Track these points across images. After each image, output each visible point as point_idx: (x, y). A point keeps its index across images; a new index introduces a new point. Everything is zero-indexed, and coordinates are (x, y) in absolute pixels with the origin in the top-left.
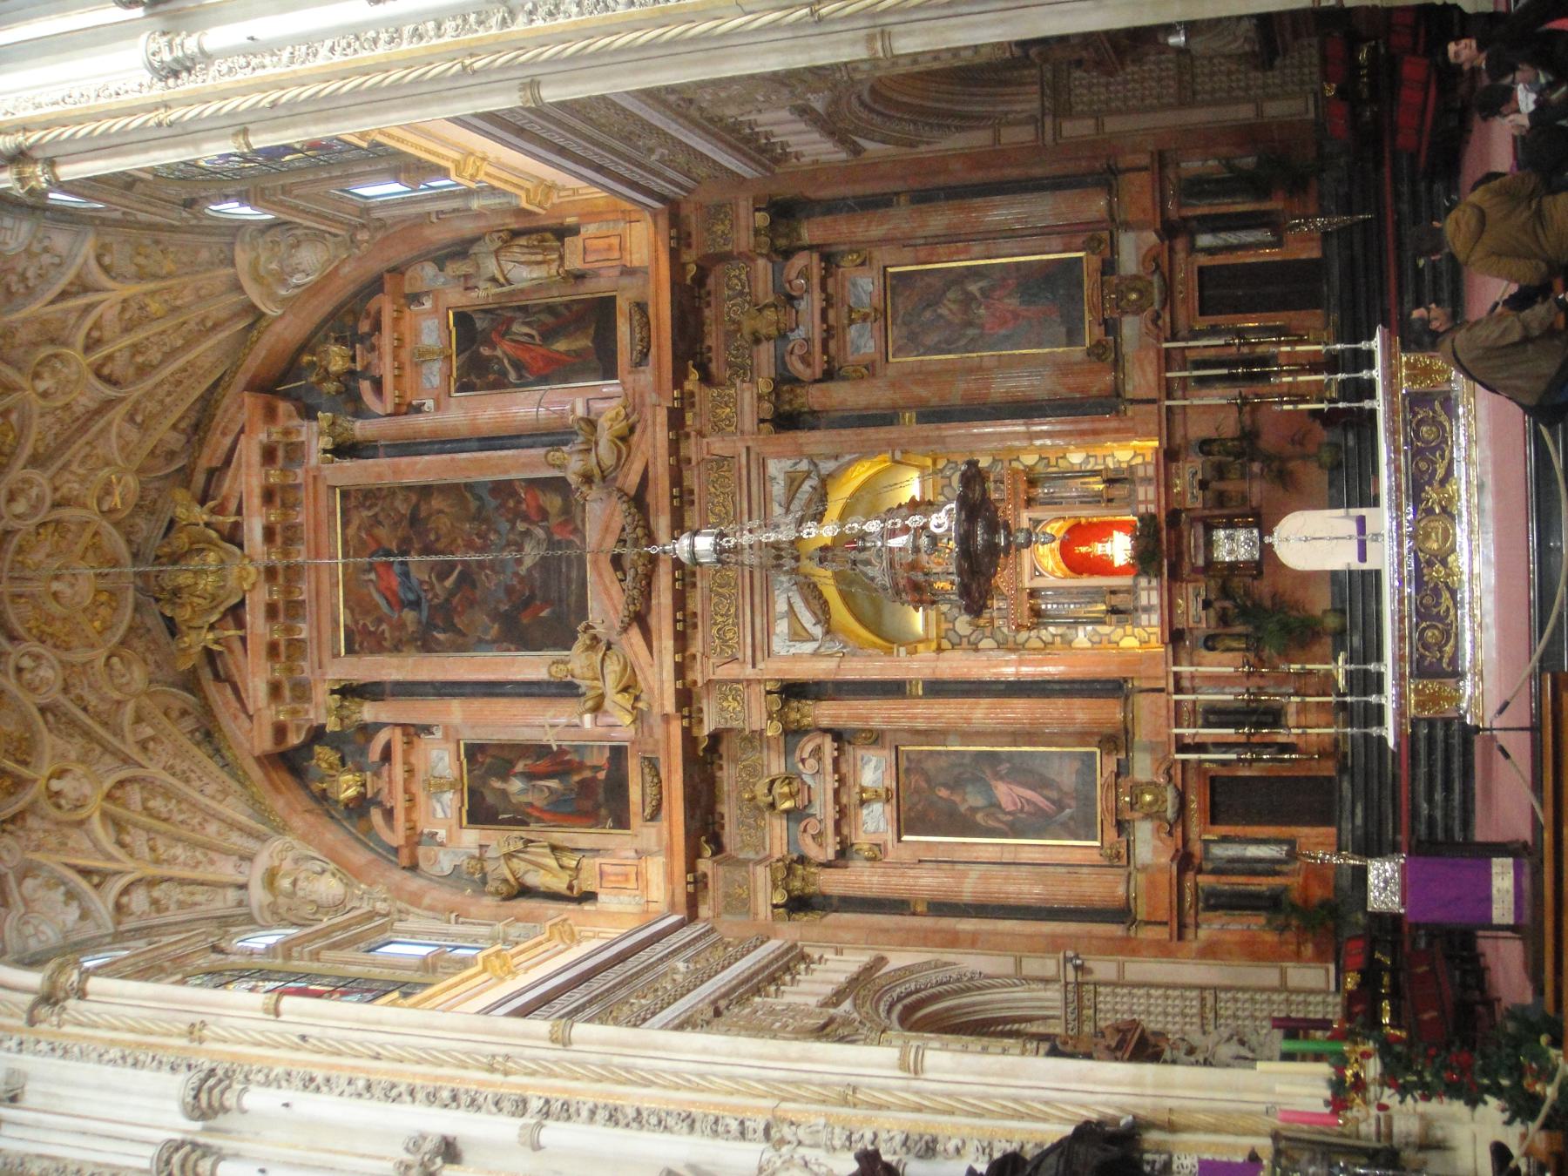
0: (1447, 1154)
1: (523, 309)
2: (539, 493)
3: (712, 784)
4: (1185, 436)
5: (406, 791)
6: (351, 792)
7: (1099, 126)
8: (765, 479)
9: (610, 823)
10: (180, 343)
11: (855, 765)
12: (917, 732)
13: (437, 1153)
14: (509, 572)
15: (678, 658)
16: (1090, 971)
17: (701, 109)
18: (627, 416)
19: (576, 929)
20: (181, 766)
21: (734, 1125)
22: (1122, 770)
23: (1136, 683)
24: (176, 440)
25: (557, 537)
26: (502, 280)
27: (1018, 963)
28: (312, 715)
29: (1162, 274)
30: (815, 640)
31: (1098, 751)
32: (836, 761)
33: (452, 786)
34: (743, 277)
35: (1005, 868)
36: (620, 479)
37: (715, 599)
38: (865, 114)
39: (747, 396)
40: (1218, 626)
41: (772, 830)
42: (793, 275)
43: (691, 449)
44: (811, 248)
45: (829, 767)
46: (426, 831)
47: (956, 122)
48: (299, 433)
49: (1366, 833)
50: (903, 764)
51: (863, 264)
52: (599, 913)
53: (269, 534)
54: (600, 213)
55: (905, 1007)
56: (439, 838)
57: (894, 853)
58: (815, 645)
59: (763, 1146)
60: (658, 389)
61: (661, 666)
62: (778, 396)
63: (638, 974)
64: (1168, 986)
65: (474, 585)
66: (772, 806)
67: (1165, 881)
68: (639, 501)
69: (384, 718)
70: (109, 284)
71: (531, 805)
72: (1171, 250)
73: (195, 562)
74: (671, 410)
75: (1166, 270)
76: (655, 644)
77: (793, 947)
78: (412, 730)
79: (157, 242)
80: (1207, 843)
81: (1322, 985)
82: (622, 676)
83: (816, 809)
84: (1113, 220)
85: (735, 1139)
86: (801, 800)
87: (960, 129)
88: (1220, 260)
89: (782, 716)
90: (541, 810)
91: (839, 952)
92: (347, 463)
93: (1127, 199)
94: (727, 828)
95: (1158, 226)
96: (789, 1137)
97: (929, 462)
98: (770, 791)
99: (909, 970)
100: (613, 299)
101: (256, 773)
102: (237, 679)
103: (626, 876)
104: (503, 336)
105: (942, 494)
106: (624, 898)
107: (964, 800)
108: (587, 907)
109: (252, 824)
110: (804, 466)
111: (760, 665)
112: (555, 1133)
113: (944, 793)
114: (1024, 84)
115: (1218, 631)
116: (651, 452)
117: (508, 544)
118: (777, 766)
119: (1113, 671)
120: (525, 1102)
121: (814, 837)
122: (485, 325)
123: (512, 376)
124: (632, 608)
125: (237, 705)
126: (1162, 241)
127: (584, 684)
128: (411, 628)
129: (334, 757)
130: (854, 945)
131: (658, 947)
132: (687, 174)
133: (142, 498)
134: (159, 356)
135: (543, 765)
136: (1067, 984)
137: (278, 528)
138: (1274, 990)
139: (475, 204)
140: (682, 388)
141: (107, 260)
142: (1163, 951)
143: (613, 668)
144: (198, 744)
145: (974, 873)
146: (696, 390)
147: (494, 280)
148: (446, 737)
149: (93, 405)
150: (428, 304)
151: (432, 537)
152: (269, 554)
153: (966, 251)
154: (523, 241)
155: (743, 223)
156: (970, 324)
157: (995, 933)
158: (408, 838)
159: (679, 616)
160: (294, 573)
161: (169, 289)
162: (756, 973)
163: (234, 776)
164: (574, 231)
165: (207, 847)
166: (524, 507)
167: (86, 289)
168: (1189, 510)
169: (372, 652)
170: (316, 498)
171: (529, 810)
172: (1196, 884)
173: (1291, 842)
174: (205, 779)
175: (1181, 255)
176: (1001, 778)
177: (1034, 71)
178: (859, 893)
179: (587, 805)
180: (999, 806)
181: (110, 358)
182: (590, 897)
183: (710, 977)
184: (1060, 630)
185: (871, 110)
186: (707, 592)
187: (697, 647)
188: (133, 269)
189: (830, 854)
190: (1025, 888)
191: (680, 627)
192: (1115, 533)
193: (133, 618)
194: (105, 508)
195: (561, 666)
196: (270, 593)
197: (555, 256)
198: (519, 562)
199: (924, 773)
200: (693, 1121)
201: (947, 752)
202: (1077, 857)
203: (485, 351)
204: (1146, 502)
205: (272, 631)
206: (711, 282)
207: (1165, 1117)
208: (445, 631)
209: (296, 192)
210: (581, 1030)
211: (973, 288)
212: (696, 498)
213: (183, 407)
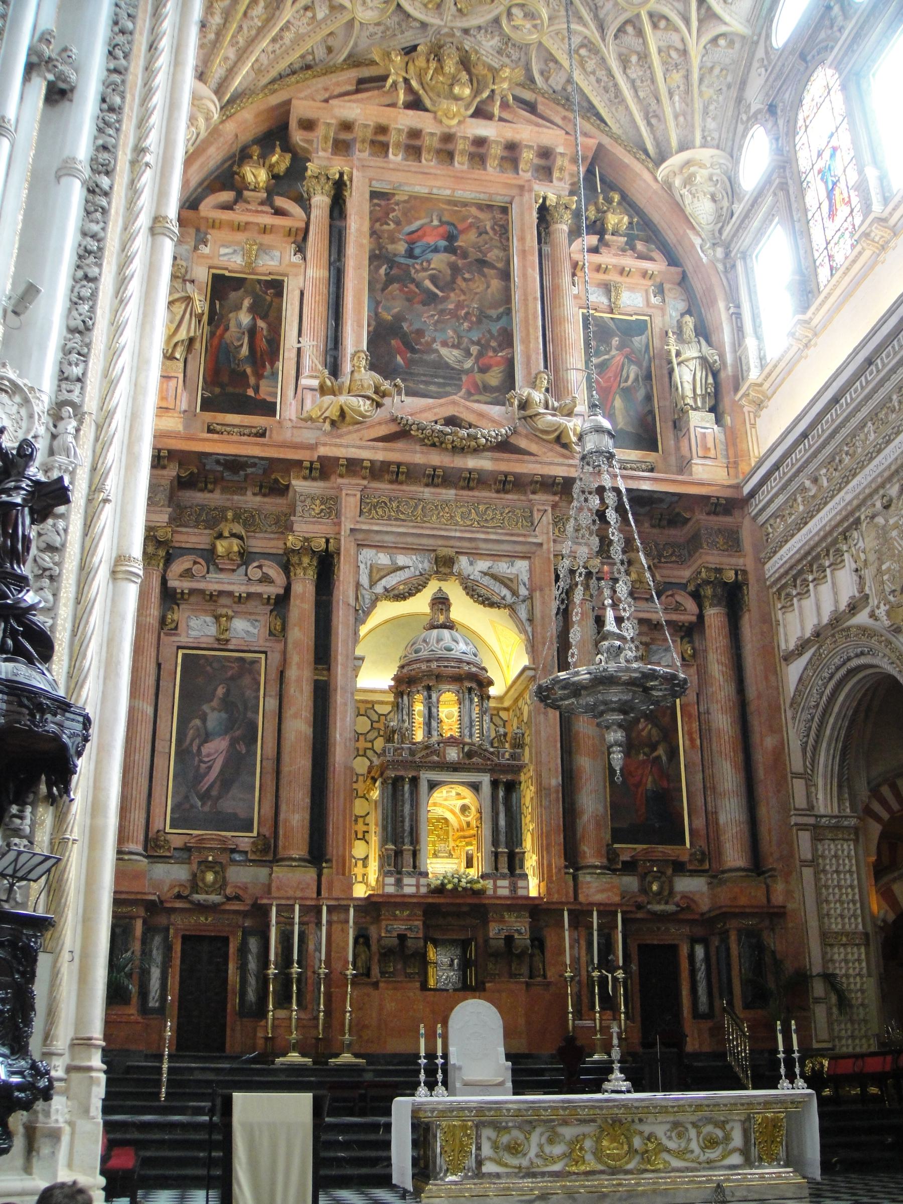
1: (648, 377)
2: (502, 368)
5: (247, 223)
6: (250, 178)
7: (805, 863)
8: (512, 557)
9: (207, 394)
10: (641, 94)
11: (251, 614)
13: (61, 77)
14: (437, 334)
15: (367, 464)
17: (873, 517)
20: (288, 36)
21: (77, 371)
23: (325, 871)
24: (557, 81)
25: (464, 378)
26: (680, 359)
28: (321, 154)
29: (676, 913)
30: (371, 587)
33: (249, 264)
34: (674, 558)
37: (412, 503)
38: (837, 661)
42: (678, 598)
44: (701, 617)
45: (254, 589)
46: (209, 237)
47: (811, 741)
48: (560, 179)
53: (480, 142)
54: (735, 445)
56: (202, 247)
65: (424, 305)
66: (220, 536)
68: (504, 446)
69: (315, 213)
70: (705, 39)
71: (227, 329)
72: (692, 922)
73: (464, 76)
75: (681, 916)
76: (380, 444)
78: (300, 238)
79: (729, 87)
82: (352, 410)
84: (724, 872)
86: (223, 563)
88: (685, 965)
92: (535, 215)
94: (199, 495)
95: (724, 910)
96: (61, 425)
97: (507, 704)
98: (233, 535)
100: (657, 451)
101: (275, 100)
102: (359, 96)
104: (627, 357)
107: (213, 709)
109: (232, 89)
110: (523, 592)
112: (76, 193)
113: (220, 691)
114: (839, 800)
115: (374, 948)
117: (460, 337)
119: (333, 849)
120: (107, 173)
122: (636, 344)
123: (595, 360)
124: (414, 427)
125: (338, 90)
126: (703, 914)
127: (345, 379)
128: (390, 247)
129: (282, 168)
132: (774, 516)
133: (514, 45)
134: (634, 76)
135: (263, 344)
137: (482, 150)
139: (750, 342)
141: (722, 42)
144: (303, 57)
145: (150, 710)
147: (678, 354)
148: (295, 265)
149: (601, 16)
150: (654, 300)
151: (467, 276)
152: (465, 138)
154: (710, 380)
155: (726, 560)
158: (207, 219)
159: (403, 469)
160: (447, 155)
161: (688, 91)
163: (273, 82)
164: (718, 421)
165: (216, 44)
166: (491, 354)
167: (700, 21)
169: (371, 212)
170: (507, 185)
171: (222, 328)
173: (161, 1011)
174: (272, 56)
175: (686, 930)
176: (233, 743)
177: (848, 810)
179: (225, 379)
181: (640, 33)
185: (838, 669)
186: (420, 496)
188: (709, 65)
189: (173, 583)
191: (393, 468)
193: (415, 19)
194: (515, 11)
196: (432, 134)
197: (699, 404)
198: (445, 344)
199: (240, 675)
200: (80, 332)
201: (258, 698)
202: (157, 811)
203: (615, 341)
204: (495, 887)
205: (399, 131)
206: (673, 532)
208: (387, 274)
209: (781, 194)
210: (168, 247)
211: (660, 751)
212: (502, 496)
213: (587, 90)
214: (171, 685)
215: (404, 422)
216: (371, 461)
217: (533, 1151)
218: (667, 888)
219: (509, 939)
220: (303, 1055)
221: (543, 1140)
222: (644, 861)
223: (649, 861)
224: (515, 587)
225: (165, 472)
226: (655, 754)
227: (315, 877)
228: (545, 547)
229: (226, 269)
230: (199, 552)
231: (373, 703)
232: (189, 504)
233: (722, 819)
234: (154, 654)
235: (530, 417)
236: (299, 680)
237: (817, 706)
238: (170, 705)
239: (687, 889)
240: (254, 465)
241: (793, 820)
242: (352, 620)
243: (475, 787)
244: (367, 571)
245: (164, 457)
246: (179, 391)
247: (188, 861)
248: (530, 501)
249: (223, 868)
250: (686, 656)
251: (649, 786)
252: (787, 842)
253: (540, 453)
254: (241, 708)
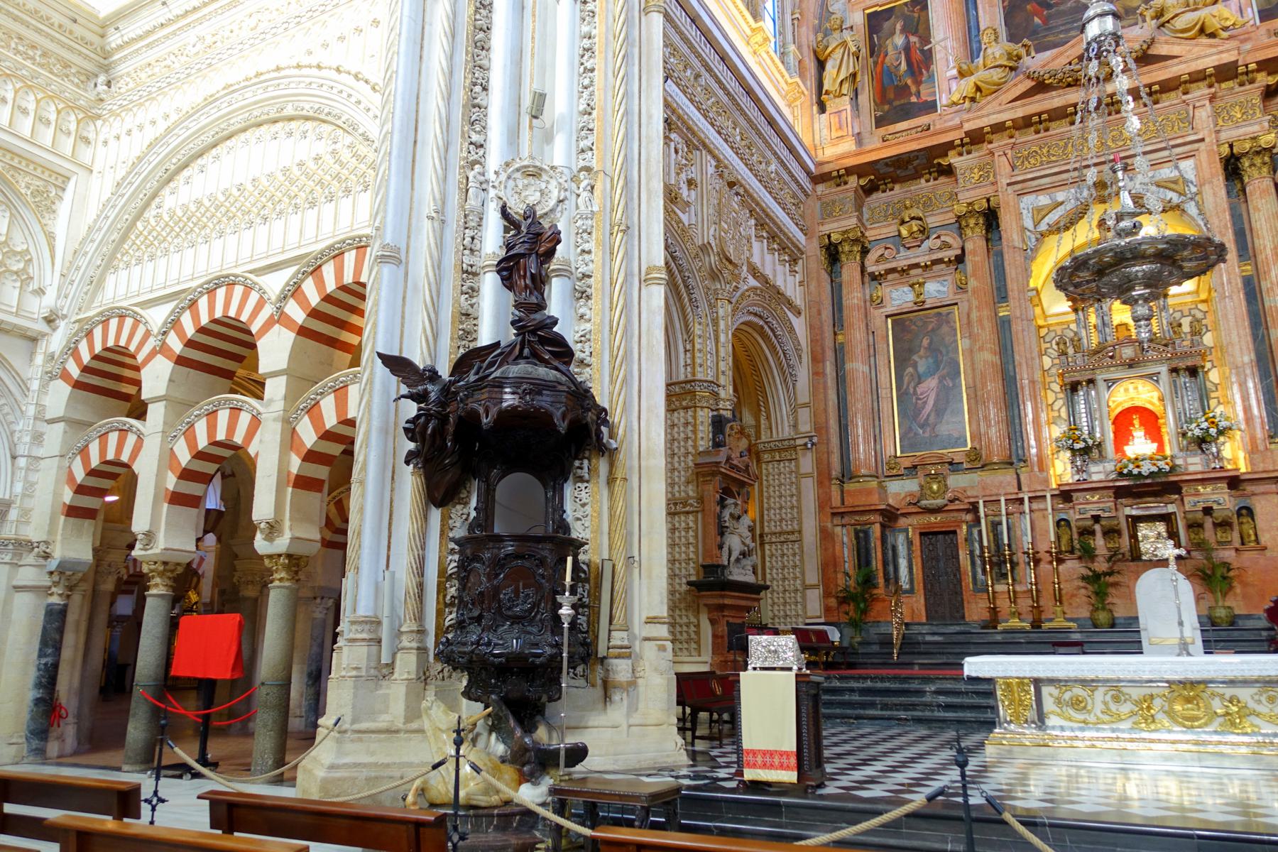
0: (601, 705)
3: (916, 176)
4: (1254, 494)
9: (879, 114)
11: (939, 276)
12: (968, 315)
15: (1009, 124)
16: (804, 455)
18: (1225, 29)
19: (798, 103)
22: (954, 466)
27: (805, 405)
30: (1035, 227)
31: (968, 448)
32: (940, 261)
35: (874, 392)
36: (1163, 38)
37: (1061, 143)
39: (1256, 128)
40: (1078, 528)
41: (885, 227)
43: (1200, 92)
45: (935, 257)
49: (919, 643)
50: (944, 310)
52: (812, 116)
55: (762, 327)
57: (878, 315)
58: (1031, 226)
59: (575, 170)
60: (1255, 50)
61: (1000, 112)
62: (1258, 153)
63: (759, 134)
64: (799, 508)
66: (903, 222)
67: (875, 501)
68: (1145, 58)
74: (1234, 64)
76: (1018, 103)
77: (802, 253)
80: (906, 531)
81: (809, 614)
83: (903, 252)
85: (578, 146)
89: (971, 213)
90: (883, 62)
91: (801, 284)
94: (884, 195)
96: (583, 185)
97: (1203, 296)
98: (913, 218)
99: (792, 330)
103: (840, 128)
105: (1174, 311)
106: (825, 132)
107: (921, 358)
108: (815, 108)
111: (1010, 189)
113: (925, 342)
115: (1074, 530)
116: (1190, 57)
118: (932, 221)
121: (882, 255)
124: (1047, 76)
127: (981, 60)
130: (807, 293)
131: (786, 152)
136: (794, 439)
138: (803, 581)
140: (1258, 71)
142: (823, 503)
143: (996, 75)
146: (1256, 85)
157: (825, 388)
162: (775, 223)
168: (1182, 500)
171: (882, 55)
172: (873, 523)
173: (911, 591)
176: (940, 382)
178: (844, 291)
179: (891, 95)
180: (919, 383)
182: (822, 108)
183: (765, 187)
184: (1064, 413)
187: (1021, 138)
189: (870, 269)
190: (859, 406)
191: (1035, 119)
195: (993, 37)
199: (939, 326)
207: (619, 475)
210: (657, 20)
214: (885, 346)
215: (1036, 75)
216: (1012, 120)
219: (1208, 511)
220: (1021, 620)
221: (1108, 698)
224: (1179, 187)
225: (847, 186)
227: (1015, 476)
228: (1207, 140)
229: (877, 5)
230: (892, 239)
231: (1068, 323)
232: (877, 205)
234: (863, 326)
235: (1168, 22)
236: (980, 321)
238: (886, 361)
240: (917, 157)
242: (1019, 258)
243: (1153, 378)
244: (1030, 215)
245: (843, 175)
246: (849, 119)
247: (915, 476)
248: (1184, 102)
249: (945, 478)
253: (1183, 54)
254: (944, 352)
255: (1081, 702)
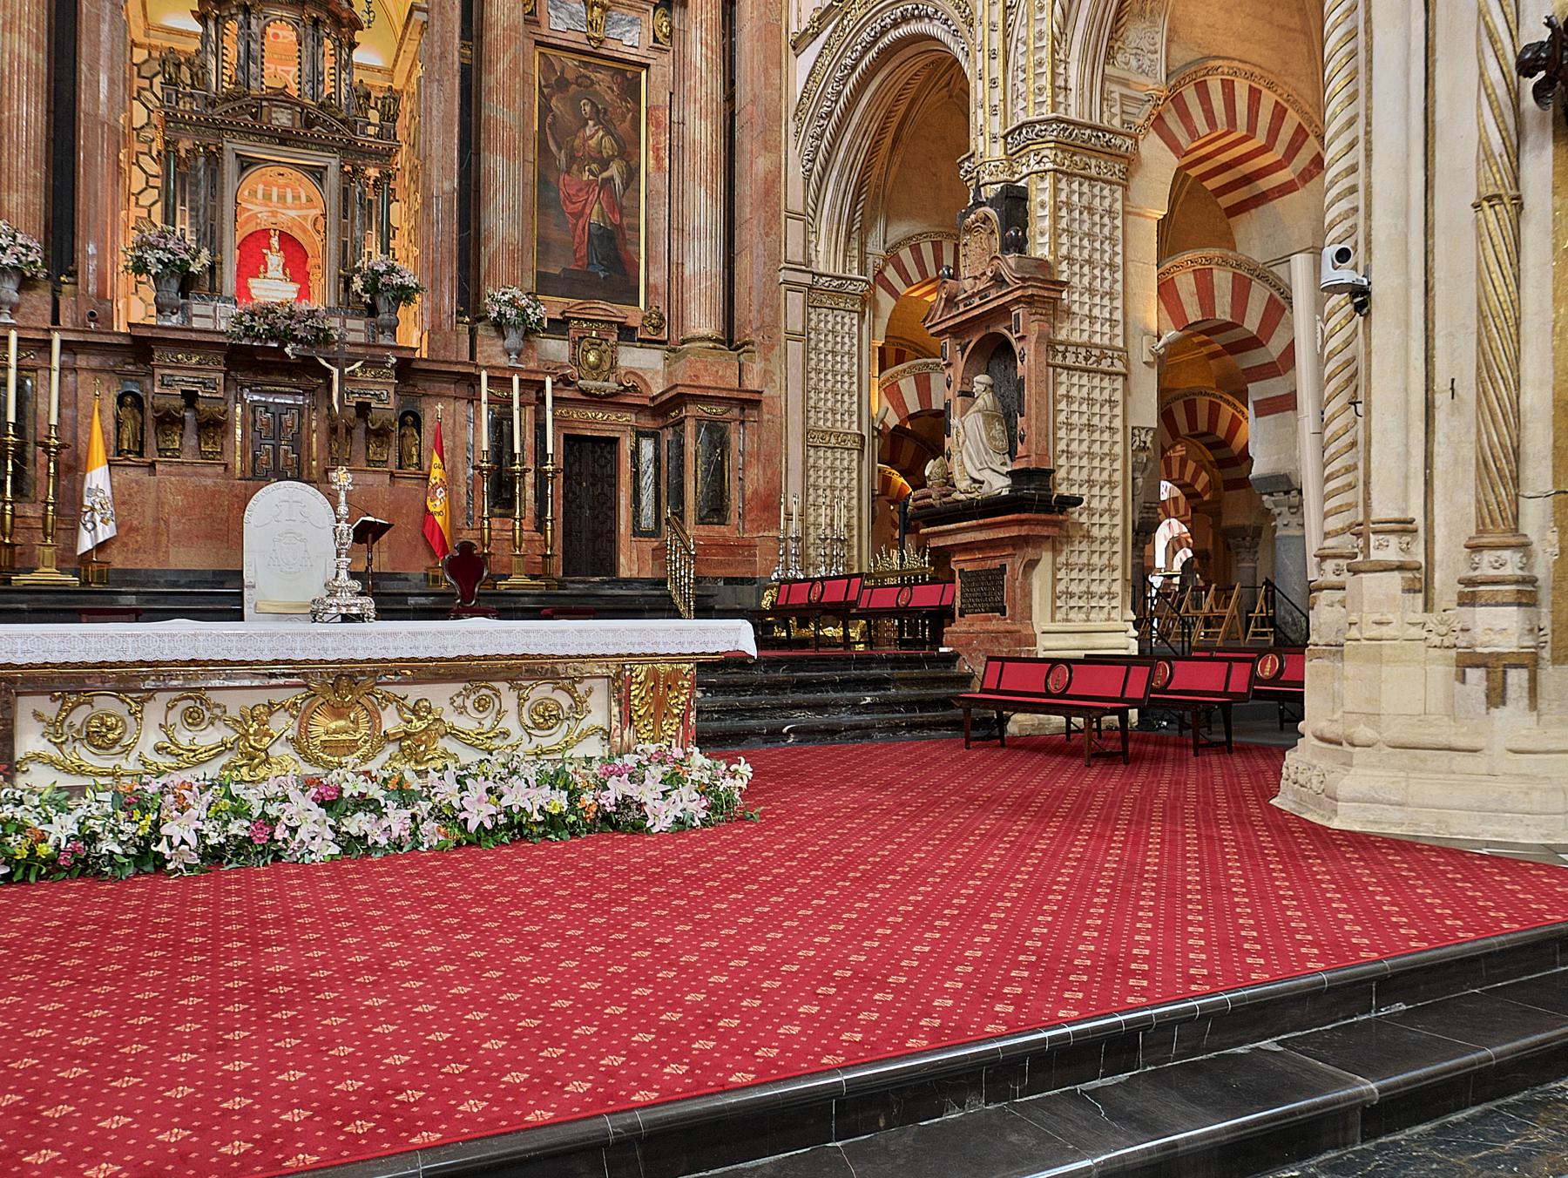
7: (792, 336)
47: (817, 168)
51: (656, 40)
87: (807, 180)
93: (710, 359)
153: (659, 168)
156: (572, 158)
185: (866, 50)
192: (295, 287)
211: (614, 171)
217: (152, 737)
218: (606, 358)
219: (363, 409)
221: (175, 716)
222: (579, 319)
223: (586, 320)
226: (605, 175)
233: (688, 270)
237: (829, 115)
239: (635, 365)
241: (782, 276)
250: (659, 35)
251: (594, 218)
252: (774, 307)
255: (110, 729)
